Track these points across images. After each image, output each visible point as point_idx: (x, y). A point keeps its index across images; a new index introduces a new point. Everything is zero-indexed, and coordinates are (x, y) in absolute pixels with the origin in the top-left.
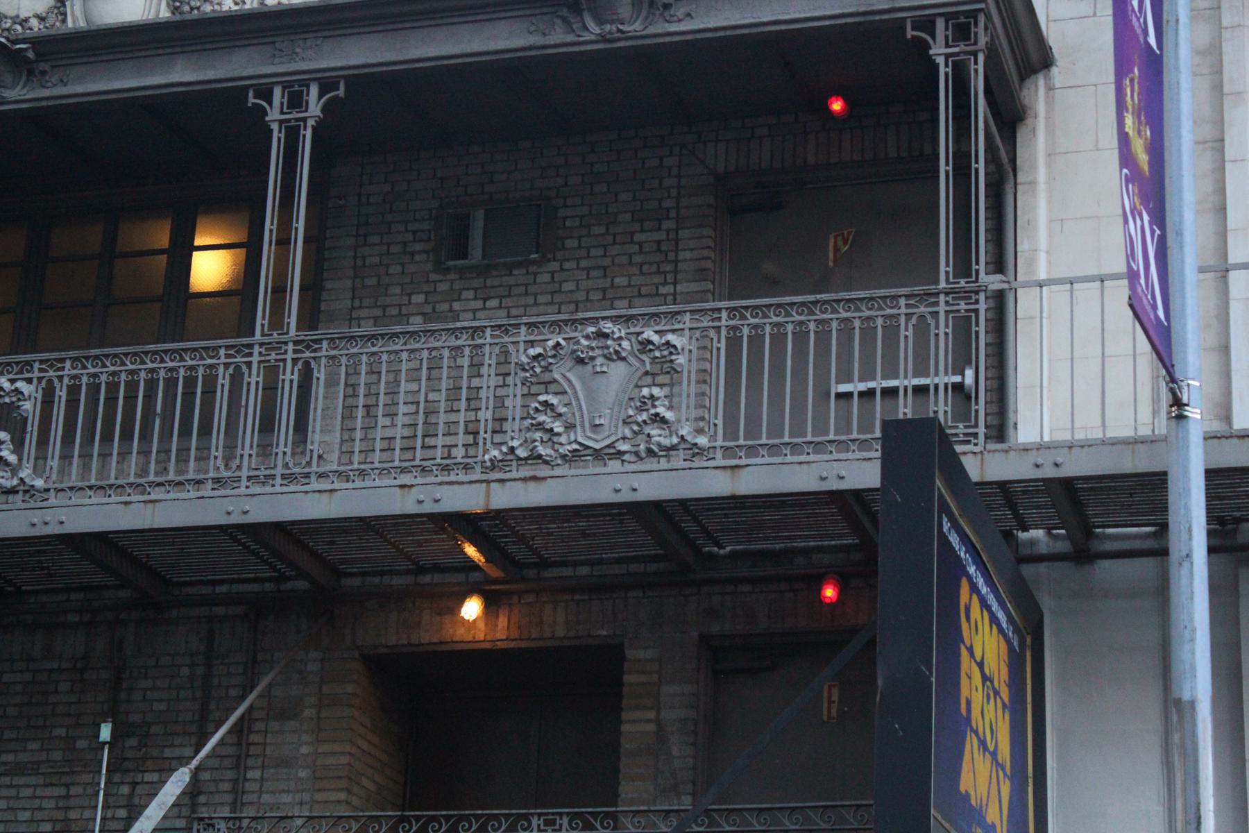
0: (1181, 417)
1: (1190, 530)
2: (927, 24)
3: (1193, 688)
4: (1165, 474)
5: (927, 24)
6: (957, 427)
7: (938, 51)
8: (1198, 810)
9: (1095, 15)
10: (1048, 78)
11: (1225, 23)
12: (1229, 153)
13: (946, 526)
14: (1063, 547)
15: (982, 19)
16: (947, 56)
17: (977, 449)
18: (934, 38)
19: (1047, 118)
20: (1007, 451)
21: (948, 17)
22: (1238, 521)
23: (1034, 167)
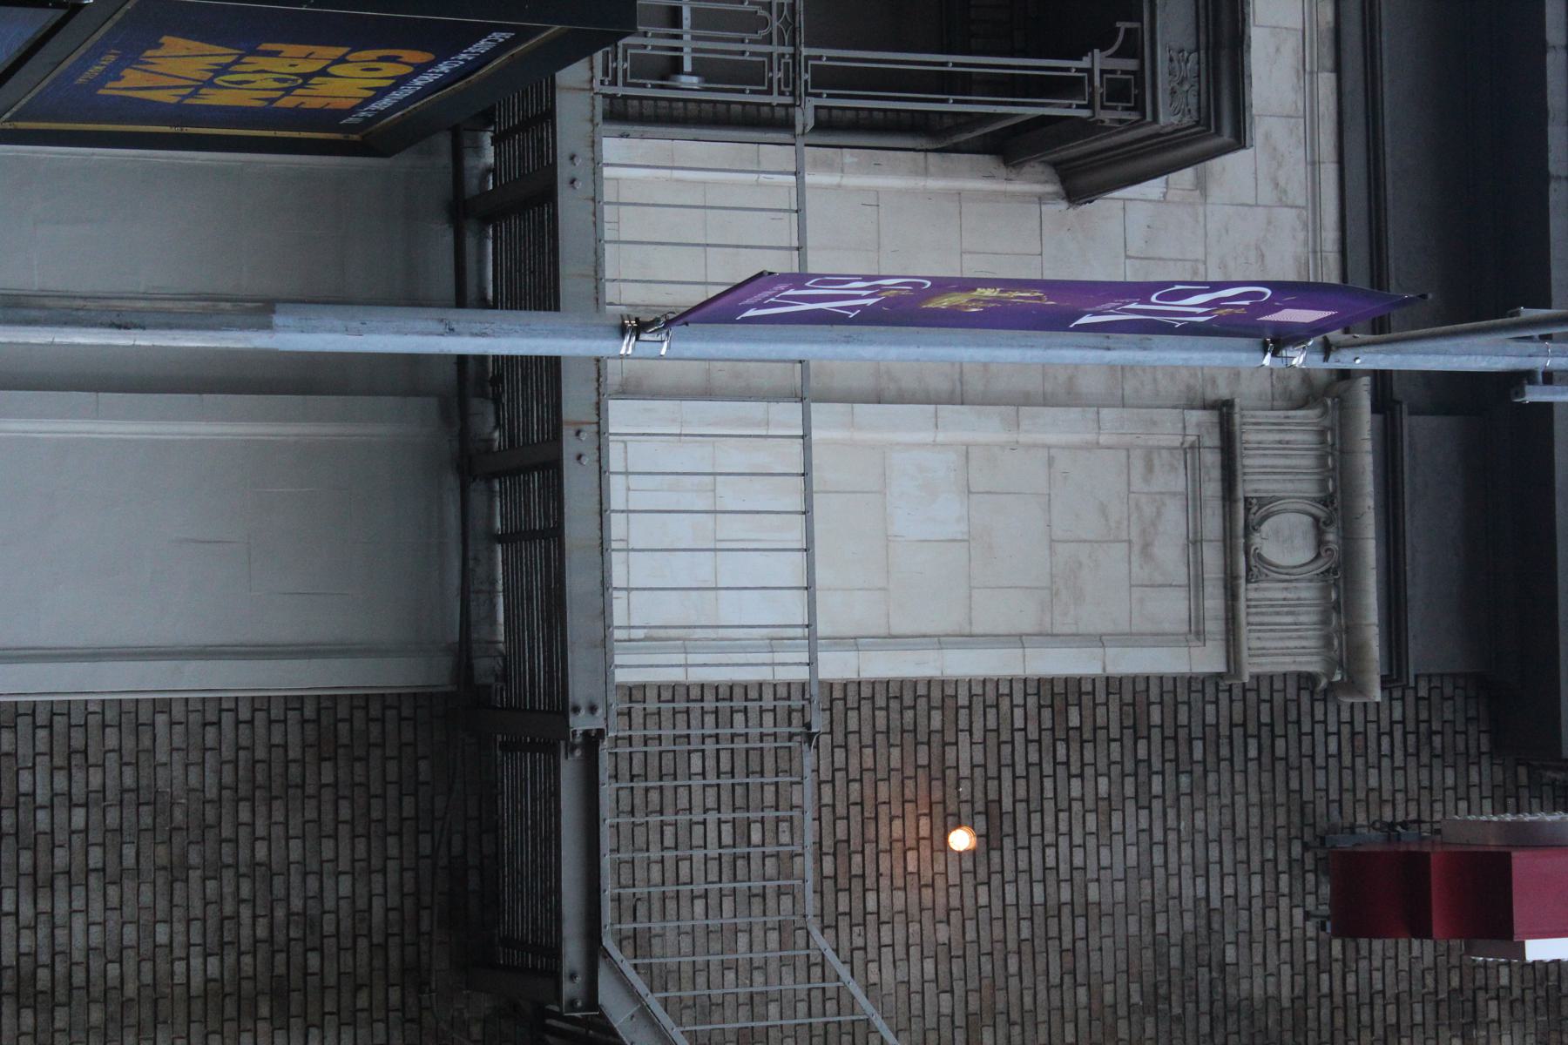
0: (623, 331)
1: (483, 335)
2: (1132, 48)
3: (286, 328)
4: (557, 309)
5: (1132, 48)
6: (625, 59)
7: (1097, 61)
8: (136, 327)
9: (1127, 257)
10: (1055, 195)
11: (1104, 412)
12: (946, 410)
13: (499, 37)
14: (472, 186)
15: (1134, 116)
16: (1090, 71)
17: (596, 83)
18: (1116, 55)
19: (1005, 193)
20: (592, 121)
21: (1138, 74)
22: (497, 400)
23: (945, 174)
